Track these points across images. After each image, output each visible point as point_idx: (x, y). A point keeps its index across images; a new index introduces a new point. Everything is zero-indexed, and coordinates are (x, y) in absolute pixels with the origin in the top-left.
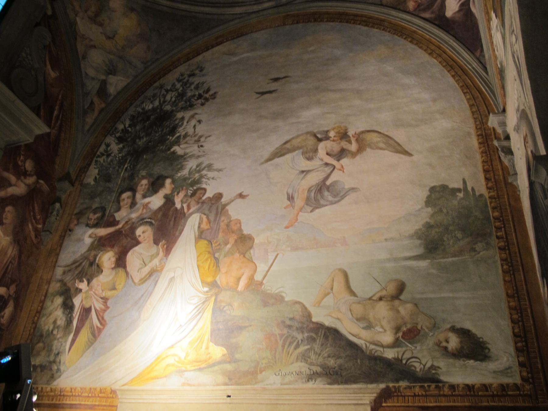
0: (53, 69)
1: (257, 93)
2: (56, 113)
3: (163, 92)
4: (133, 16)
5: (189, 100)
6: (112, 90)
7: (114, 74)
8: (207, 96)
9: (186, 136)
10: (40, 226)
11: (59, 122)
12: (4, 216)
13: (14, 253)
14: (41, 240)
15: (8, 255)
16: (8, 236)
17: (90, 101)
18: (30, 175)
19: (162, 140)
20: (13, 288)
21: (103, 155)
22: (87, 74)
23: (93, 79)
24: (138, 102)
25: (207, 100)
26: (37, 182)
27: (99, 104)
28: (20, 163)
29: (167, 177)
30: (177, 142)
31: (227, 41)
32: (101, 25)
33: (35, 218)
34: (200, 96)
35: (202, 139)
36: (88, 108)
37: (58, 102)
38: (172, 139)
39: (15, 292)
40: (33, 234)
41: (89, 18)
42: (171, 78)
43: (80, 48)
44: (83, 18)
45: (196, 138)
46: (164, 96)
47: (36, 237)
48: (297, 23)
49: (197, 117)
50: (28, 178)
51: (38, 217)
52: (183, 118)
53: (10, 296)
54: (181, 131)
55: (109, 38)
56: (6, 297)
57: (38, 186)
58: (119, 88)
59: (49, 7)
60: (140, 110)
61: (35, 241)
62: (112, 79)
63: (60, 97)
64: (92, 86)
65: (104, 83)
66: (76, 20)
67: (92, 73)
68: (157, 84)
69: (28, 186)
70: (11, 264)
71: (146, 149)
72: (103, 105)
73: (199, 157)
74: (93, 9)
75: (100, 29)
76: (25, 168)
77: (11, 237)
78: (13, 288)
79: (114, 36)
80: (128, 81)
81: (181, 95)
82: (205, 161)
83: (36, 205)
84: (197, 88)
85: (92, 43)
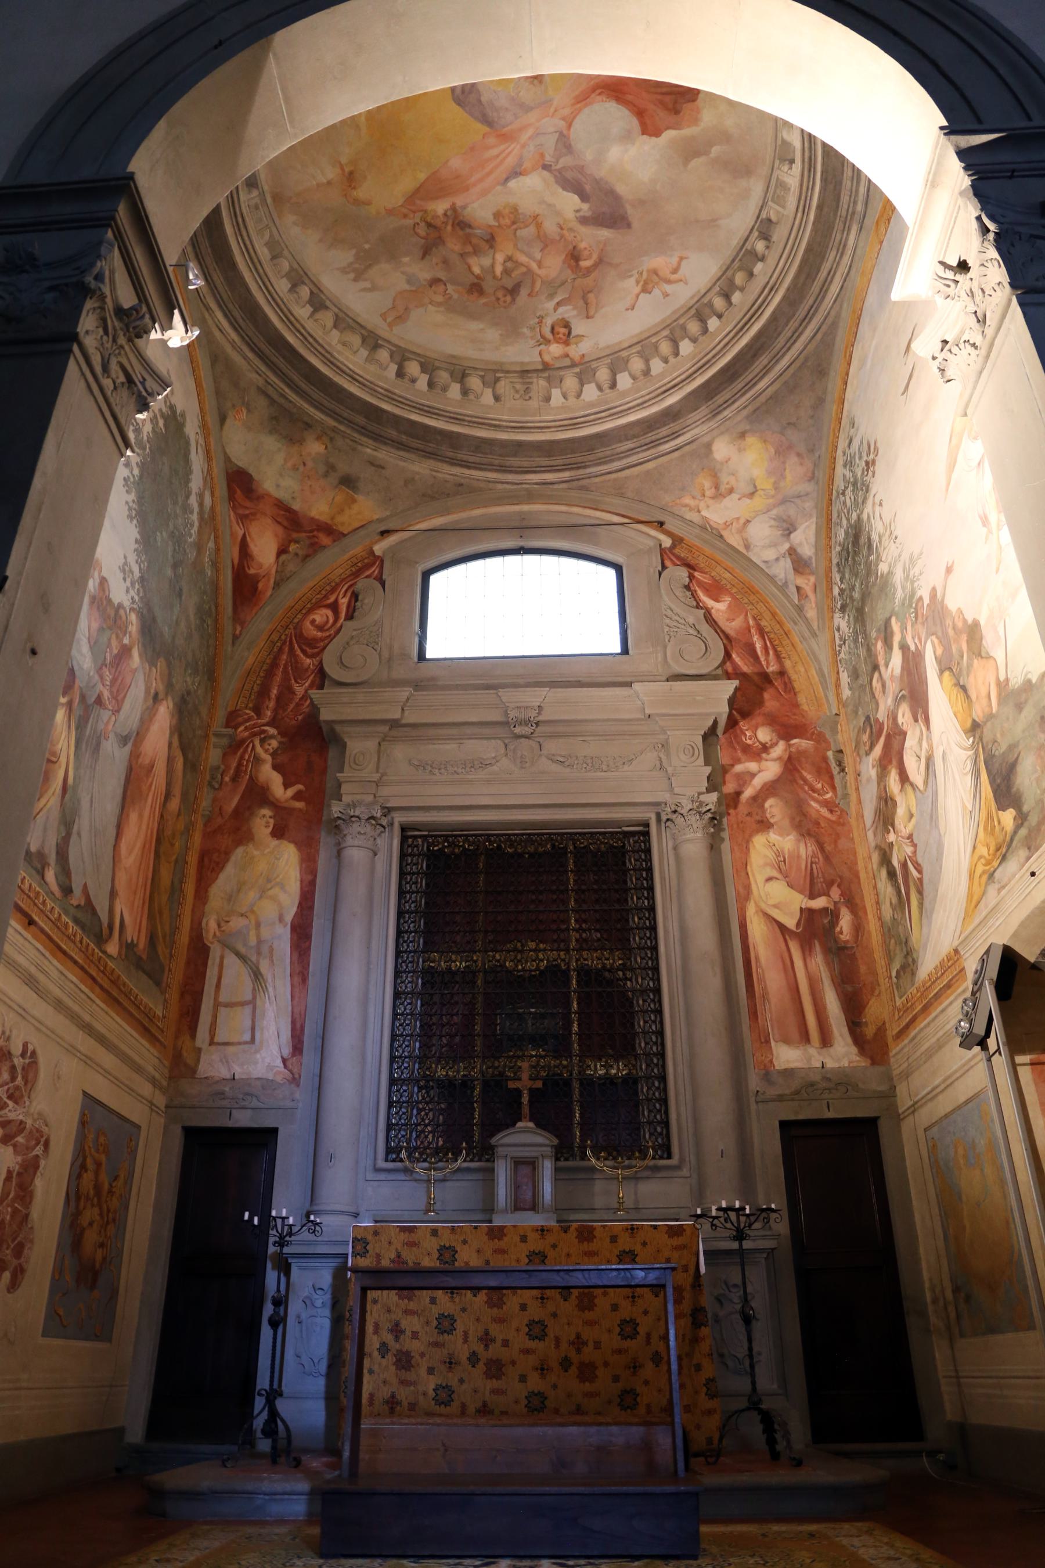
0: (717, 601)
1: (903, 394)
2: (758, 646)
3: (842, 498)
4: (750, 440)
5: (863, 484)
6: (807, 551)
7: (795, 530)
8: (872, 456)
9: (880, 537)
10: (828, 796)
11: (771, 652)
12: (768, 816)
13: (810, 849)
14: (842, 811)
15: (804, 856)
16: (788, 835)
17: (794, 590)
18: (776, 744)
19: (869, 573)
20: (835, 893)
21: (840, 646)
22: (766, 562)
23: (777, 559)
24: (833, 540)
25: (874, 462)
26: (790, 746)
27: (806, 583)
28: (749, 742)
29: (890, 618)
30: (879, 558)
31: (853, 346)
32: (731, 491)
33: (814, 791)
34: (867, 463)
35: (893, 528)
36: (799, 600)
37: (753, 631)
38: (873, 558)
39: (841, 895)
40: (824, 812)
41: (713, 498)
42: (840, 470)
43: (734, 540)
44: (708, 507)
45: (888, 533)
46: (844, 503)
47: (831, 811)
48: (889, 220)
49: (877, 501)
50: (772, 750)
51: (819, 786)
52: (869, 517)
53: (835, 903)
54: (875, 537)
55: (751, 495)
56: (832, 907)
57: (793, 750)
58: (812, 540)
59: (662, 537)
60: (838, 549)
61: (833, 818)
62: (797, 537)
63: (751, 622)
64: (783, 570)
65: (792, 552)
66: (703, 517)
67: (770, 554)
68: (834, 493)
69: (779, 759)
70: (814, 866)
71: (865, 596)
72: (812, 579)
73: (900, 556)
74: (707, 484)
75: (735, 496)
76: (760, 743)
77: (794, 833)
78: (835, 893)
79: (755, 487)
80: (814, 519)
81: (855, 484)
82: (905, 556)
83: (805, 774)
84: (860, 458)
85: (742, 521)
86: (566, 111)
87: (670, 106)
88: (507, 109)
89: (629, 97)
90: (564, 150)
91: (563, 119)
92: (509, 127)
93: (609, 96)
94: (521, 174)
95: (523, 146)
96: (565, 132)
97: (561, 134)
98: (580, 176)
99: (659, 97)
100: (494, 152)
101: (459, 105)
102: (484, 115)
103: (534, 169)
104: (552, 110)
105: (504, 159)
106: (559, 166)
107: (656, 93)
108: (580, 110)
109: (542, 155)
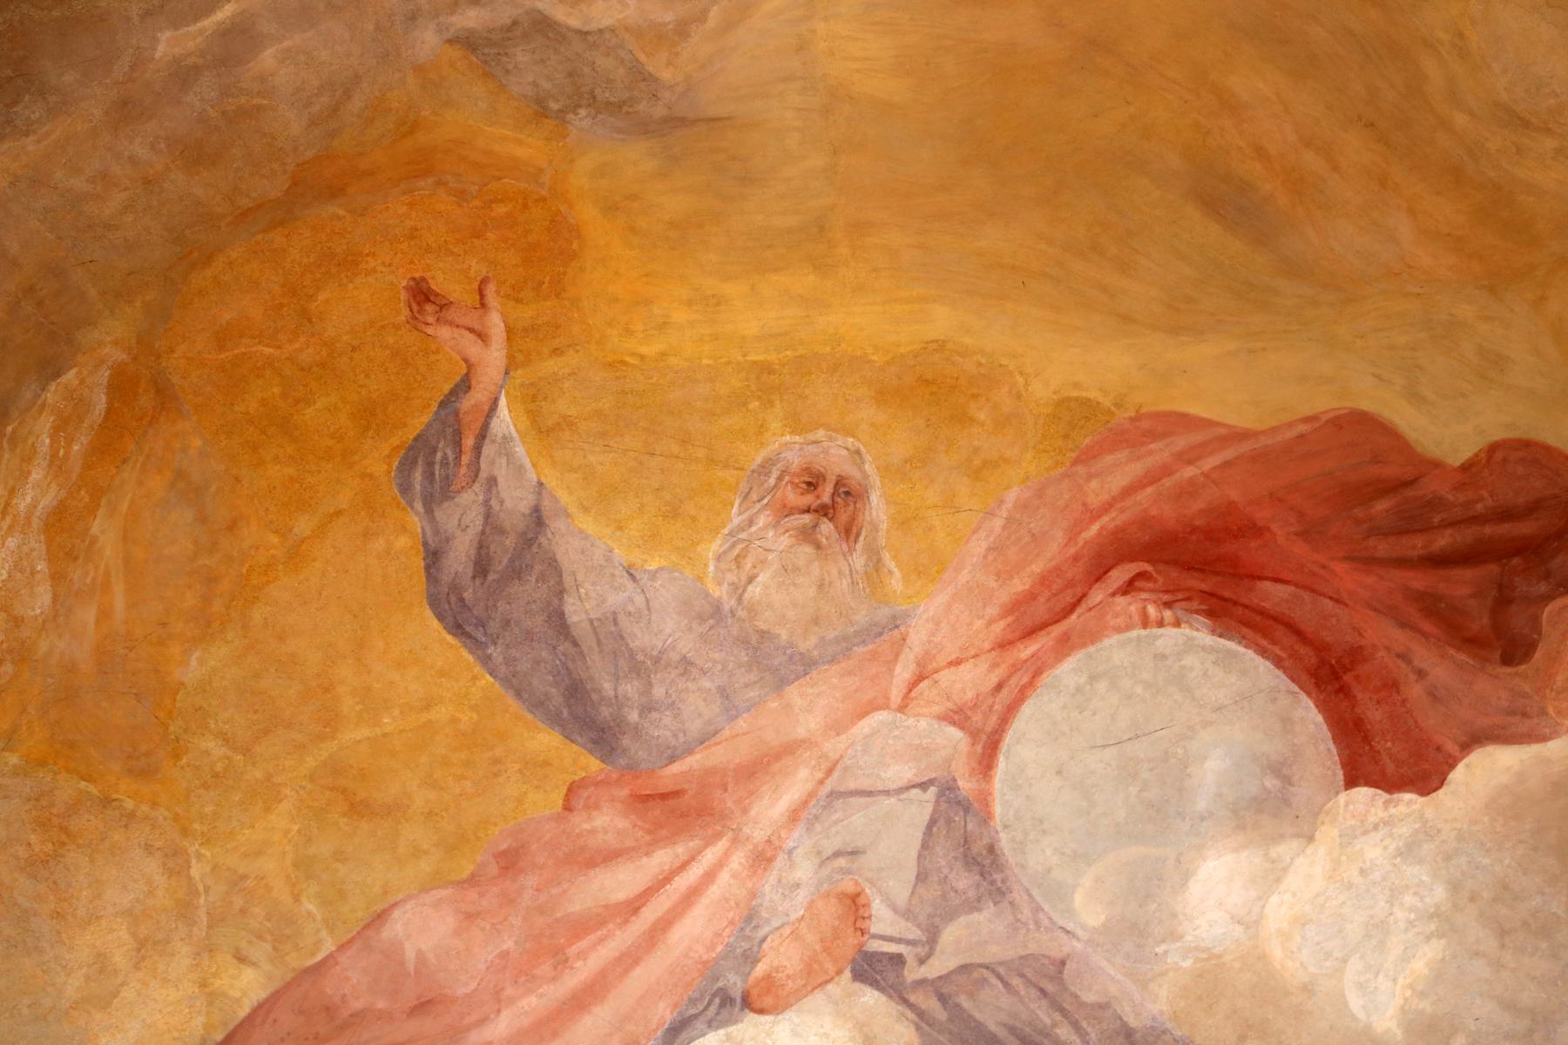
86: (970, 680)
87: (1480, 622)
88: (686, 666)
89: (1274, 595)
90: (964, 881)
91: (957, 717)
92: (694, 762)
93: (1173, 598)
94: (749, 1003)
95: (762, 859)
96: (966, 785)
97: (947, 789)
98: (1045, 1015)
99: (1419, 581)
100: (619, 882)
101: (458, 629)
102: (576, 691)
103: (813, 979)
104: (903, 672)
105: (665, 924)
106: (936, 968)
107: (1402, 563)
108: (1037, 670)
109: (854, 905)
